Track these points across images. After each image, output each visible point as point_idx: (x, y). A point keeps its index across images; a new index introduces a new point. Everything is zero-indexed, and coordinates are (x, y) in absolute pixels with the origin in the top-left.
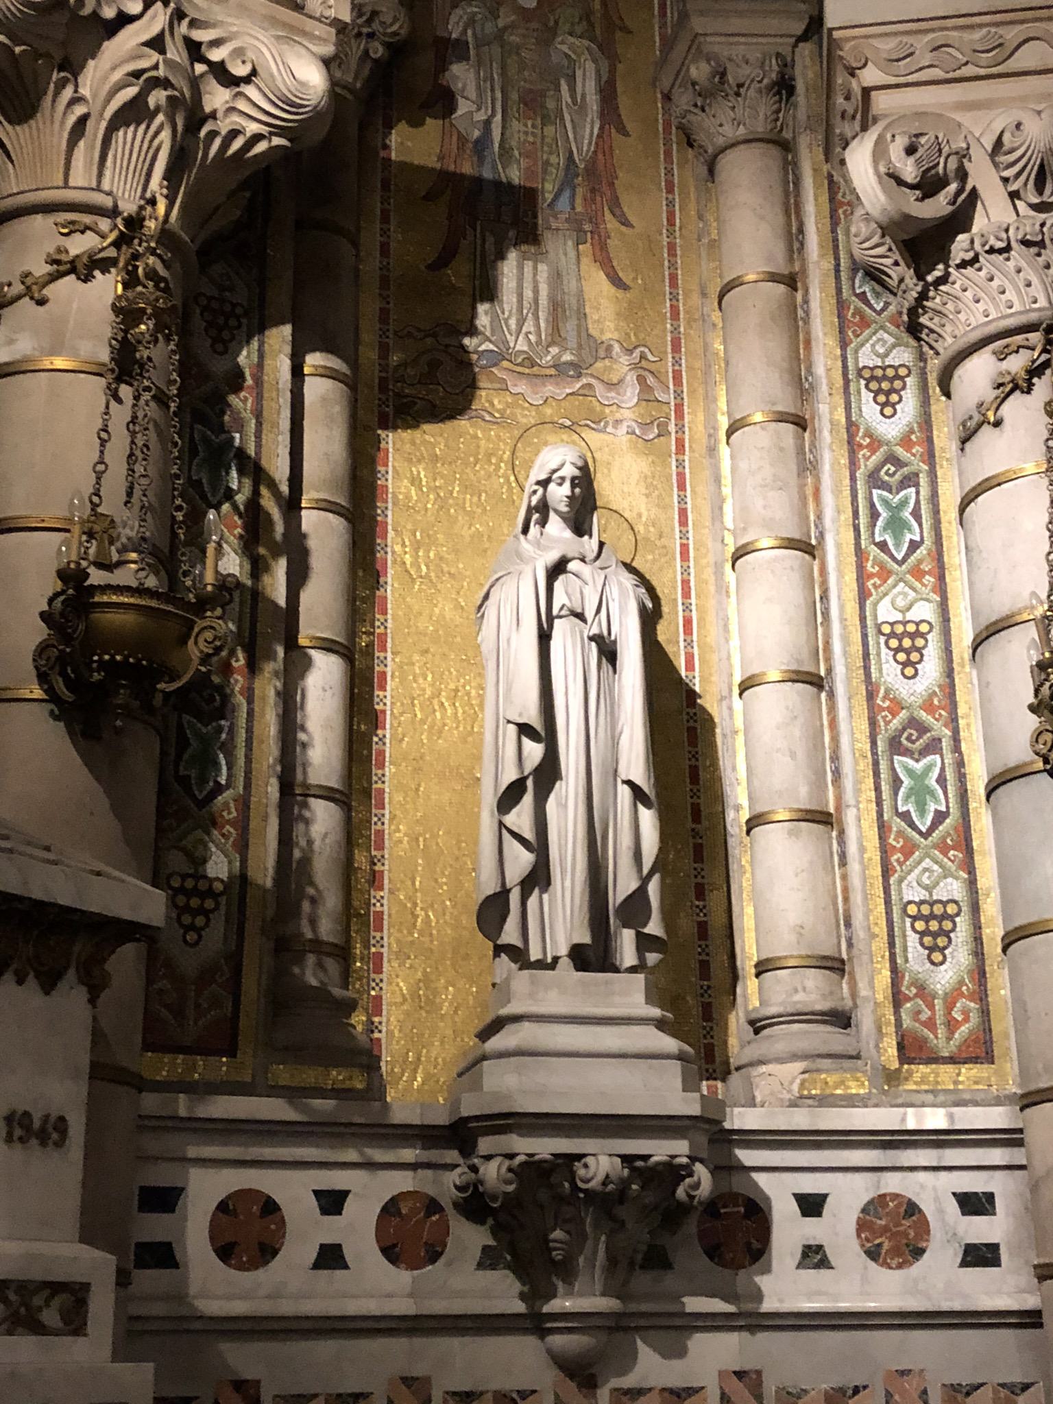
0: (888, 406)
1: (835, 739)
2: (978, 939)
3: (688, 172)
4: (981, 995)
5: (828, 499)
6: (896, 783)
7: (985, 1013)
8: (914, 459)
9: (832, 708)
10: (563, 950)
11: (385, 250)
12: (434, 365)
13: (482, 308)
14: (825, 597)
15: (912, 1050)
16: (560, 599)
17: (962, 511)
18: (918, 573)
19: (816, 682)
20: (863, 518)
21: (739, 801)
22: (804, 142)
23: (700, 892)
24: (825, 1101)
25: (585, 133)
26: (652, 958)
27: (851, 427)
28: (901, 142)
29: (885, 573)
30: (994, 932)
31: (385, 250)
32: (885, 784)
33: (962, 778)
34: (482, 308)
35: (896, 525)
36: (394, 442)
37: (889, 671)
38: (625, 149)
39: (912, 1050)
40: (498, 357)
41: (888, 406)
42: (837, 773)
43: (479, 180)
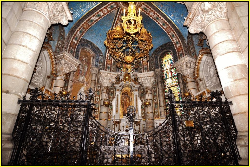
0: (99, 88)
8: (99, 91)
37: (96, 100)
38: (88, 72)
41: (99, 88)
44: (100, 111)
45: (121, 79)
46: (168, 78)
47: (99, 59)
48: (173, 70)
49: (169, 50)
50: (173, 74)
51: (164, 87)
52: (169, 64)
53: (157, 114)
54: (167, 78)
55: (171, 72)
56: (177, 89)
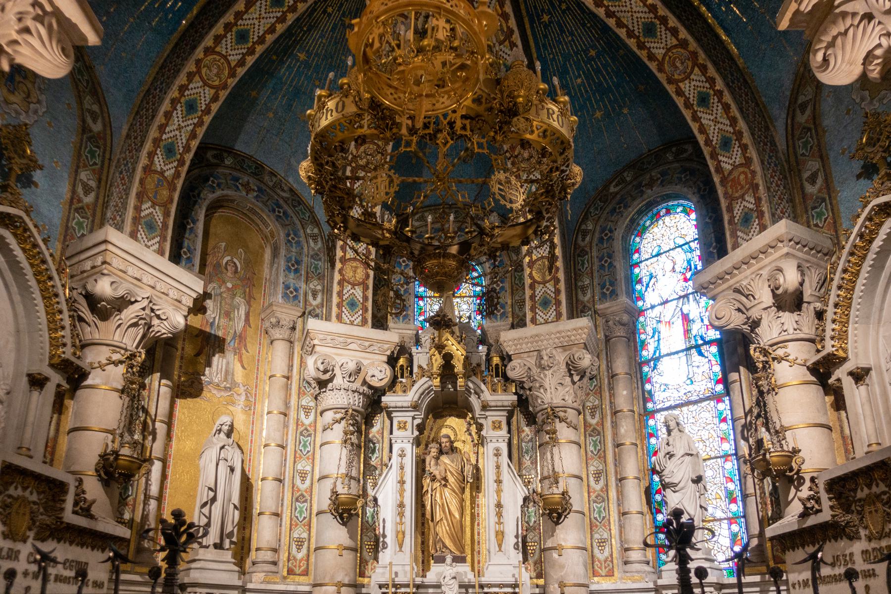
1: (283, 496)
2: (309, 548)
3: (265, 341)
4: (308, 560)
5: (290, 437)
6: (296, 509)
7: (308, 565)
9: (283, 488)
10: (212, 543)
11: (183, 349)
12: (193, 382)
13: (207, 369)
14: (285, 460)
15: (290, 572)
16: (222, 455)
17: (321, 446)
18: (308, 458)
19: (280, 481)
20: (297, 442)
21: (256, 509)
22: (296, 344)
23: (244, 529)
24: (268, 583)
25: (240, 325)
26: (233, 546)
27: (298, 419)
28: (321, 361)
29: (301, 457)
30: (313, 546)
31: (183, 349)
32: (293, 509)
33: (311, 510)
34: (207, 369)
35: (305, 446)
36: (179, 402)
37: (298, 482)
38: (250, 332)
39: (290, 572)
40: (210, 383)
42: (282, 505)
43: (211, 334)
44: (317, 541)
45: (420, 367)
46: (668, 355)
47: (305, 259)
51: (645, 401)
52: (674, 270)
53: (607, 553)
54: (664, 352)
55: (686, 318)
56: (716, 421)
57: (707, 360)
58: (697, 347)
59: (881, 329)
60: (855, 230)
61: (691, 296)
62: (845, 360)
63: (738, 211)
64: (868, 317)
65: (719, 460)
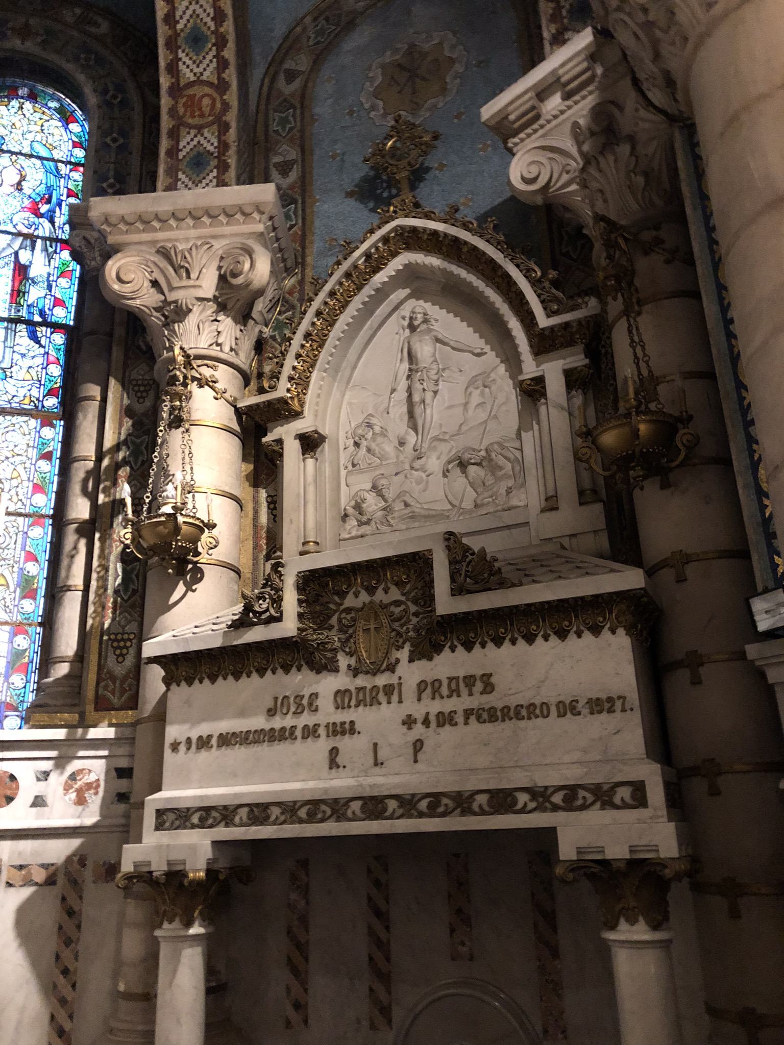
48: (39, 266)
49: (69, 67)
50: (35, 294)
52: (19, 186)
55: (21, 271)
56: (33, 453)
57: (42, 351)
58: (29, 323)
59: (348, 394)
60: (364, 247)
61: (39, 242)
62: (297, 415)
63: (187, 143)
64: (337, 371)
65: (20, 520)
